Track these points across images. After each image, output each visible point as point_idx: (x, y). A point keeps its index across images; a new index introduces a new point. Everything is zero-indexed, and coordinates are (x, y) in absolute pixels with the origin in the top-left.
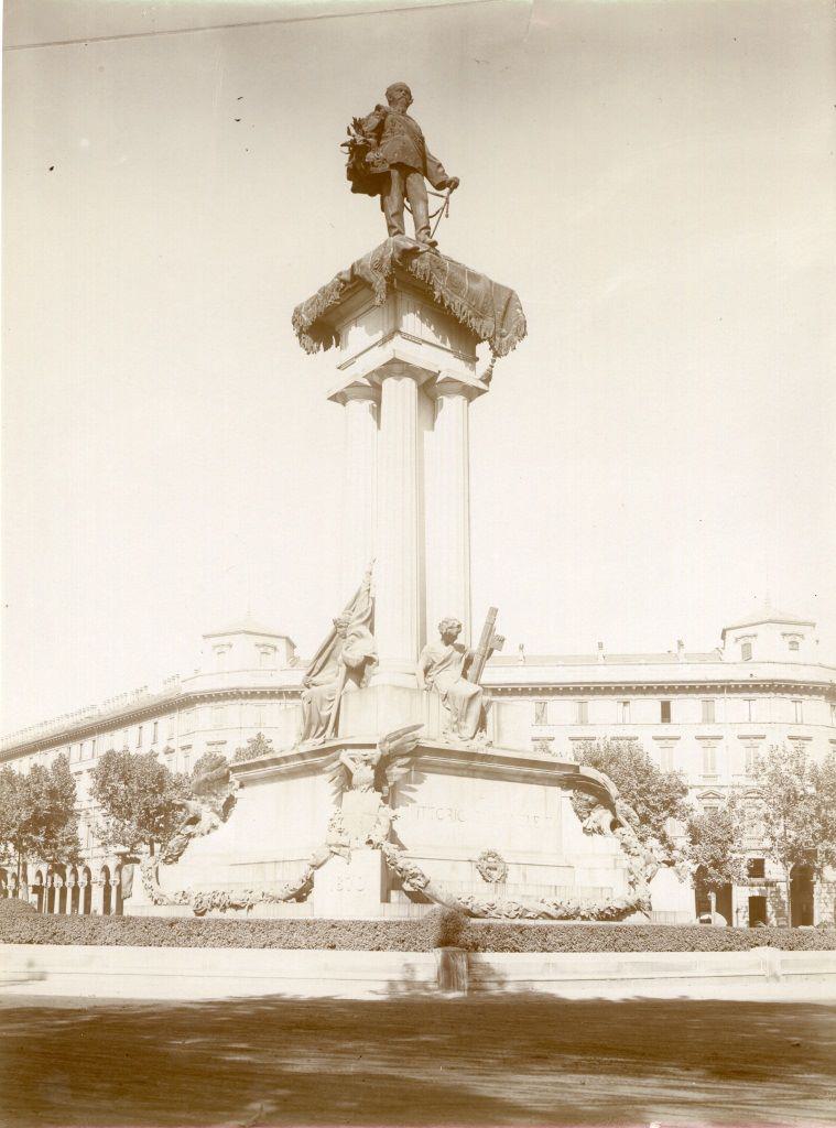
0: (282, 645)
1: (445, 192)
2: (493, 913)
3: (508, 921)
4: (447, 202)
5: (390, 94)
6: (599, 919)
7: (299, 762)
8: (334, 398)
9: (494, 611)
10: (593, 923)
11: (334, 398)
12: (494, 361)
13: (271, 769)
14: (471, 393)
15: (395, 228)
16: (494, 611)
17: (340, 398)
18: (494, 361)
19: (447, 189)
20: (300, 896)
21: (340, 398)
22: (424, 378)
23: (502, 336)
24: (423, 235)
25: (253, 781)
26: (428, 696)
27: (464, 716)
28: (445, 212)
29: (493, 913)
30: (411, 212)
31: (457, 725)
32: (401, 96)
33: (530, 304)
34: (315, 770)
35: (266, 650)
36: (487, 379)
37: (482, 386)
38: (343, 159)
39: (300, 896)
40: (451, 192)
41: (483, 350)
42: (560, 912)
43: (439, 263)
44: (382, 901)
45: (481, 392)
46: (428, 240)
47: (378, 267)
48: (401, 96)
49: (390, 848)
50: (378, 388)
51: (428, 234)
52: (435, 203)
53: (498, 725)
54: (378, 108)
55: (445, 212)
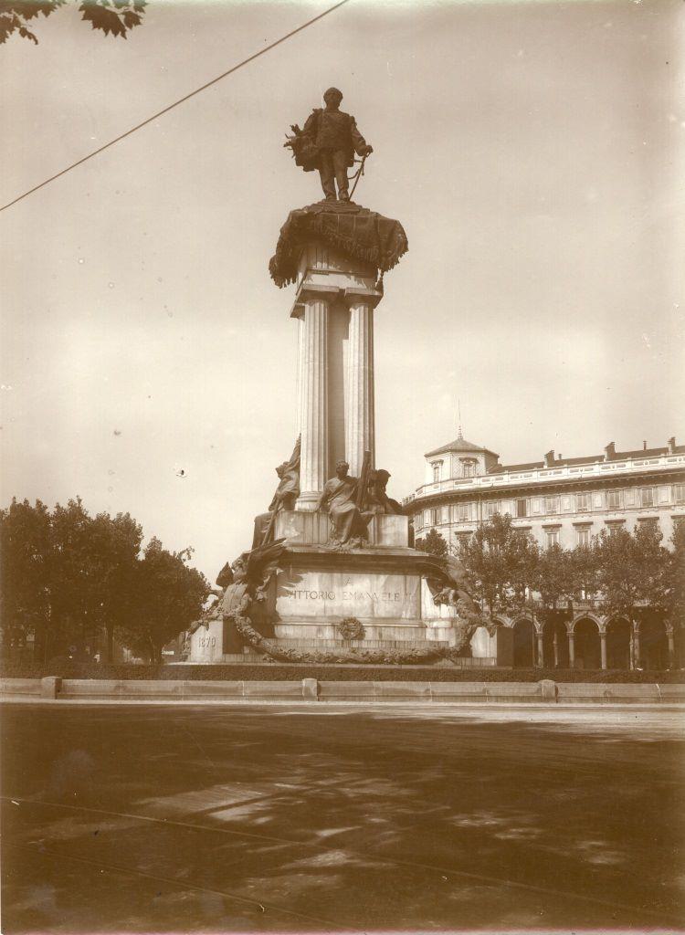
0: (481, 459)
2: (307, 660)
3: (318, 665)
4: (363, 166)
6: (400, 663)
10: (396, 666)
23: (387, 256)
26: (318, 519)
29: (307, 660)
31: (336, 535)
35: (468, 462)
37: (377, 293)
42: (365, 659)
44: (224, 653)
45: (379, 298)
53: (378, 531)
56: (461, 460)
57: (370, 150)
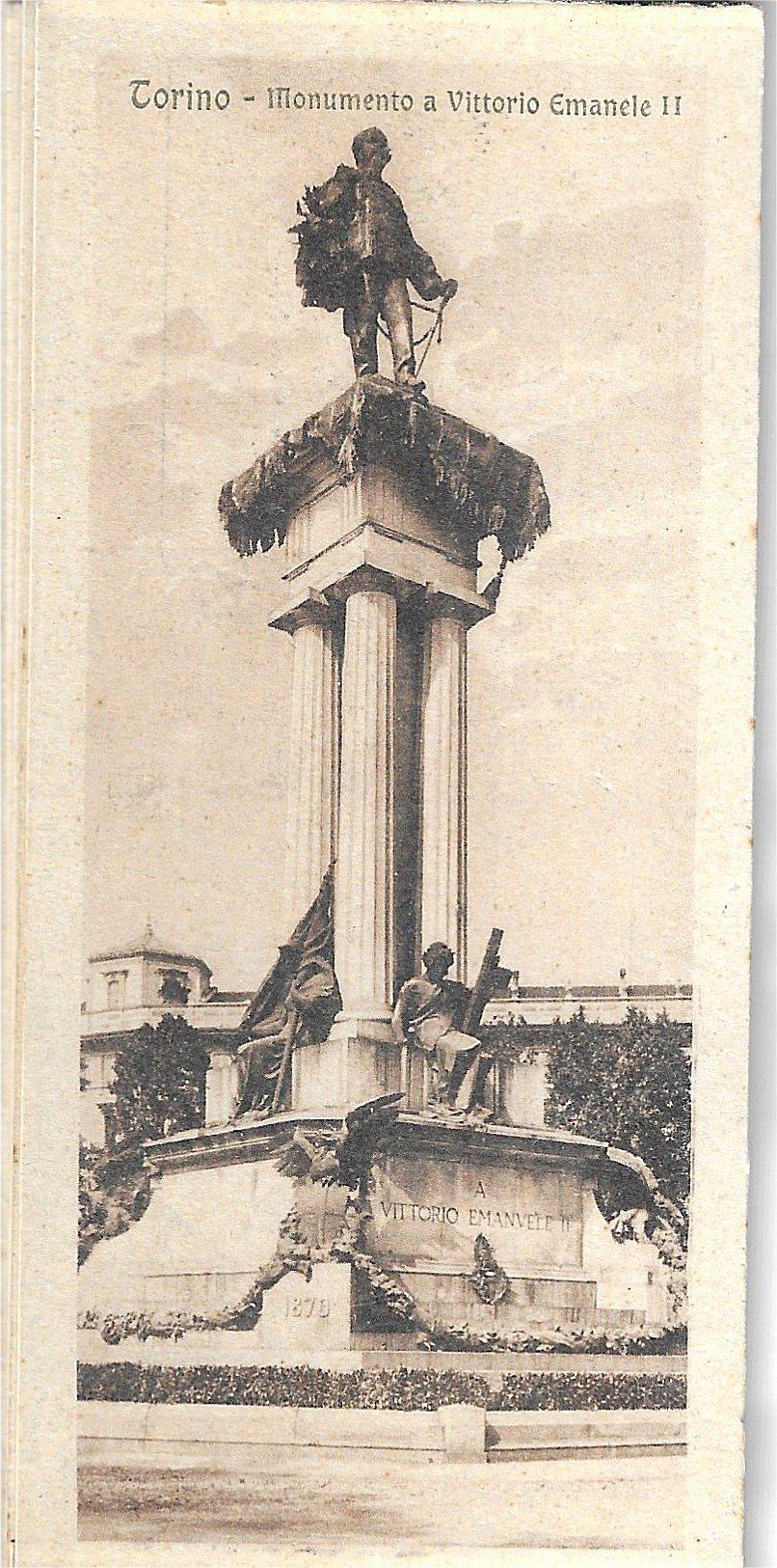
1: (435, 304)
5: (357, 147)
7: (237, 1144)
8: (277, 624)
9: (497, 935)
11: (277, 624)
12: (503, 566)
13: (199, 1151)
14: (469, 616)
15: (365, 355)
16: (497, 935)
17: (286, 624)
18: (503, 566)
19: (440, 299)
20: (246, 1318)
21: (286, 624)
22: (405, 592)
24: (405, 375)
25: (174, 1166)
27: (455, 1081)
28: (436, 336)
30: (388, 336)
32: (372, 148)
33: (557, 484)
34: (258, 1154)
36: (493, 591)
38: (285, 251)
39: (246, 1318)
40: (446, 300)
41: (489, 549)
43: (430, 416)
46: (412, 381)
47: (342, 426)
48: (372, 148)
49: (363, 1260)
50: (341, 607)
51: (412, 371)
52: (423, 320)
54: (342, 168)
55: (436, 336)
56: (161, 971)
57: (448, 289)
